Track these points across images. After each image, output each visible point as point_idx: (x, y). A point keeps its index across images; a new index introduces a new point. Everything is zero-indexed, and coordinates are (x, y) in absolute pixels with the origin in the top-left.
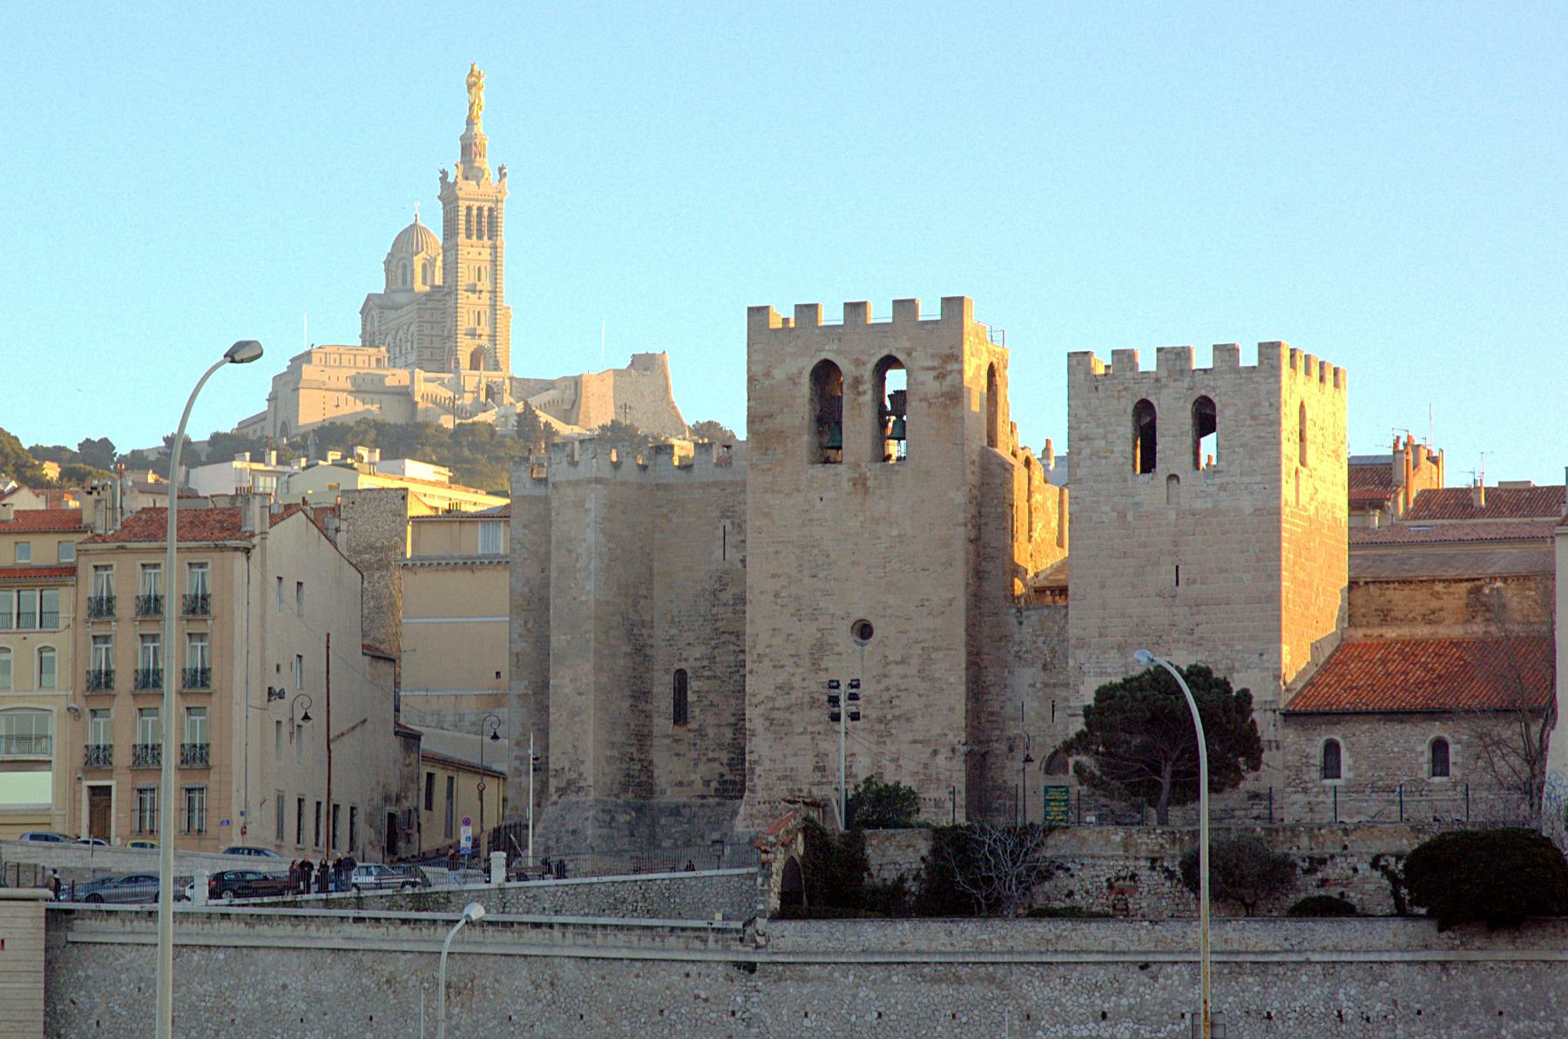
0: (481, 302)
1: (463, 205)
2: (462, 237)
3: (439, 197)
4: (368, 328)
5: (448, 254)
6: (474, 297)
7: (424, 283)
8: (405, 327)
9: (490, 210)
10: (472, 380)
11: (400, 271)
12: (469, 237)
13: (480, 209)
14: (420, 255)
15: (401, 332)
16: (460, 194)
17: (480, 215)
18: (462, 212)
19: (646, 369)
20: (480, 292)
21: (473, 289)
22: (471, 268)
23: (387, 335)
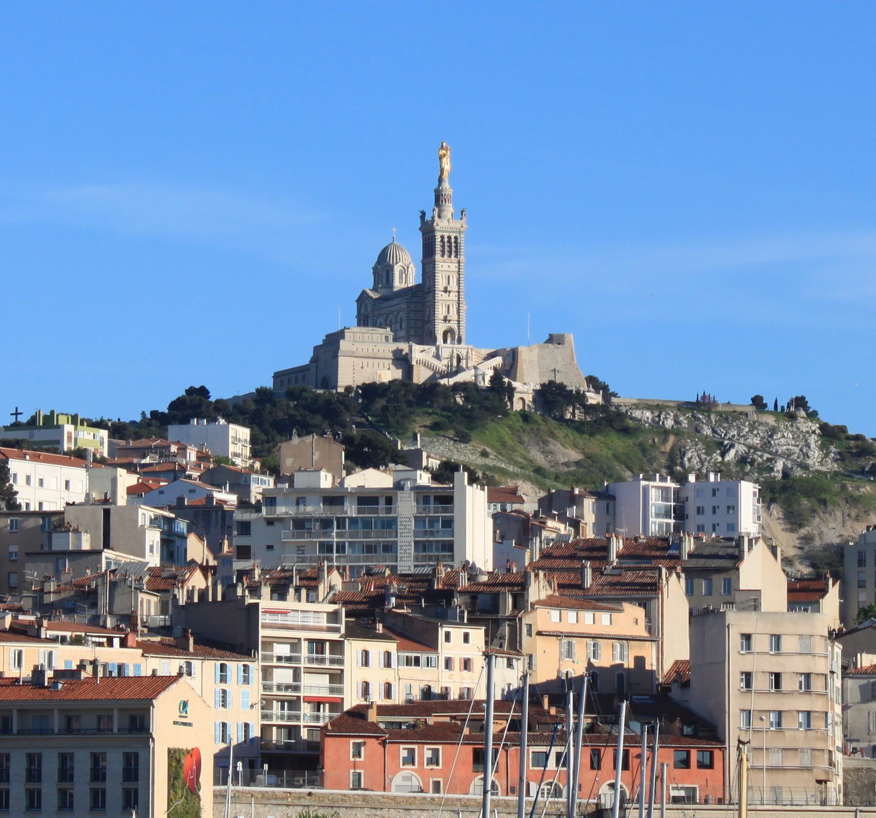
0: (450, 298)
1: (438, 235)
2: (438, 257)
3: (420, 229)
4: (363, 311)
5: (427, 266)
6: (445, 296)
7: (401, 282)
8: (395, 313)
9: (456, 238)
10: (446, 350)
11: (384, 275)
12: (443, 256)
13: (449, 237)
14: (398, 264)
15: (390, 316)
16: (437, 228)
17: (449, 241)
18: (438, 239)
19: (559, 344)
20: (450, 292)
21: (446, 290)
22: (444, 276)
23: (379, 317)
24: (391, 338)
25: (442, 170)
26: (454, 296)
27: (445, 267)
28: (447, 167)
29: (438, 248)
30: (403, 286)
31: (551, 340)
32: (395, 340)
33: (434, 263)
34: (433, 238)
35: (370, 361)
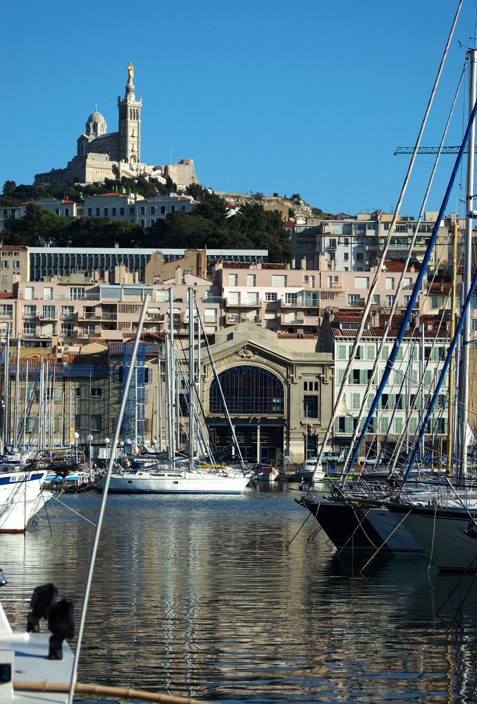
1: (129, 108)
2: (129, 119)
6: (132, 139)
16: (129, 105)
24: (108, 159)
25: (130, 76)
26: (135, 139)
27: (132, 125)
28: (132, 73)
29: (129, 115)
30: (102, 133)
31: (182, 162)
32: (111, 160)
33: (126, 122)
34: (126, 110)
35: (100, 170)
